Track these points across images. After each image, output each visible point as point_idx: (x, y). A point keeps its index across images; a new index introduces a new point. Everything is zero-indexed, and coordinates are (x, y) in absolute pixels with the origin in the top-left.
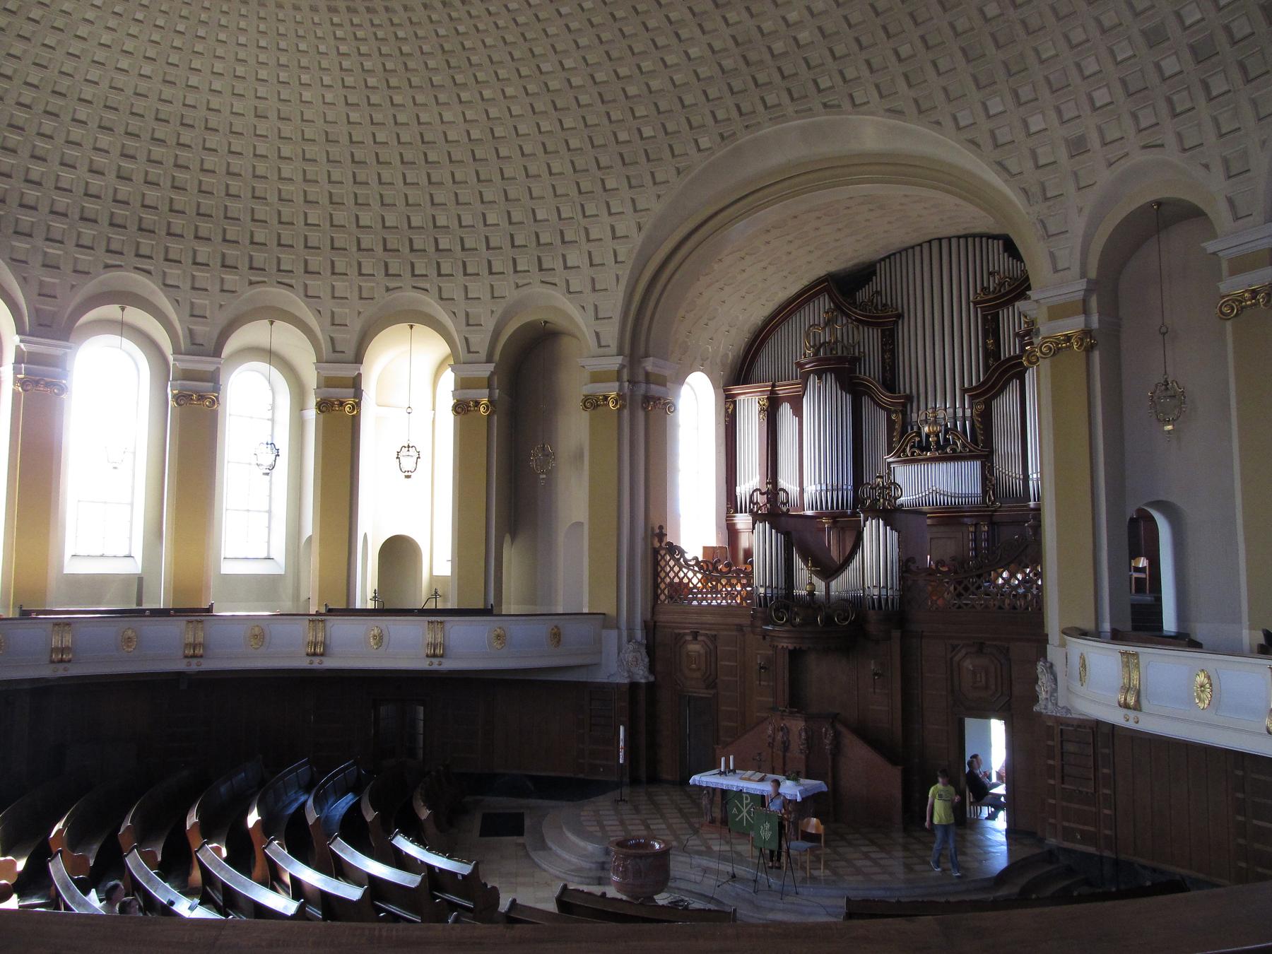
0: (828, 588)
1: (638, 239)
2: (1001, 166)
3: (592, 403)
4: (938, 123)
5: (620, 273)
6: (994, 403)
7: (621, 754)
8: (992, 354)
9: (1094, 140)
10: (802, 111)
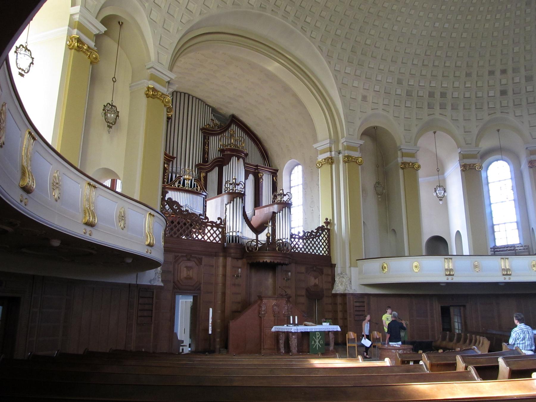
0: (257, 237)
1: (197, 19)
2: (340, 90)
3: (152, 94)
4: (330, 62)
5: (180, 28)
6: (208, 174)
7: (210, 328)
8: (205, 153)
9: (370, 99)
10: (294, 22)
